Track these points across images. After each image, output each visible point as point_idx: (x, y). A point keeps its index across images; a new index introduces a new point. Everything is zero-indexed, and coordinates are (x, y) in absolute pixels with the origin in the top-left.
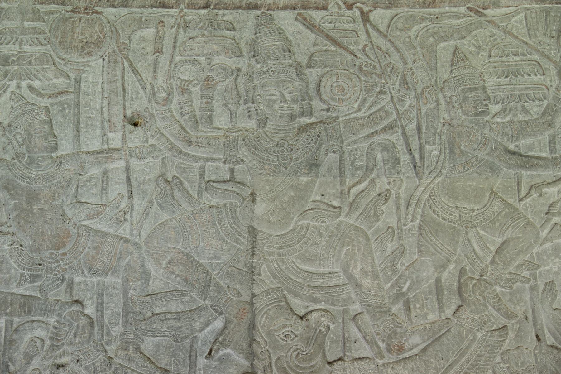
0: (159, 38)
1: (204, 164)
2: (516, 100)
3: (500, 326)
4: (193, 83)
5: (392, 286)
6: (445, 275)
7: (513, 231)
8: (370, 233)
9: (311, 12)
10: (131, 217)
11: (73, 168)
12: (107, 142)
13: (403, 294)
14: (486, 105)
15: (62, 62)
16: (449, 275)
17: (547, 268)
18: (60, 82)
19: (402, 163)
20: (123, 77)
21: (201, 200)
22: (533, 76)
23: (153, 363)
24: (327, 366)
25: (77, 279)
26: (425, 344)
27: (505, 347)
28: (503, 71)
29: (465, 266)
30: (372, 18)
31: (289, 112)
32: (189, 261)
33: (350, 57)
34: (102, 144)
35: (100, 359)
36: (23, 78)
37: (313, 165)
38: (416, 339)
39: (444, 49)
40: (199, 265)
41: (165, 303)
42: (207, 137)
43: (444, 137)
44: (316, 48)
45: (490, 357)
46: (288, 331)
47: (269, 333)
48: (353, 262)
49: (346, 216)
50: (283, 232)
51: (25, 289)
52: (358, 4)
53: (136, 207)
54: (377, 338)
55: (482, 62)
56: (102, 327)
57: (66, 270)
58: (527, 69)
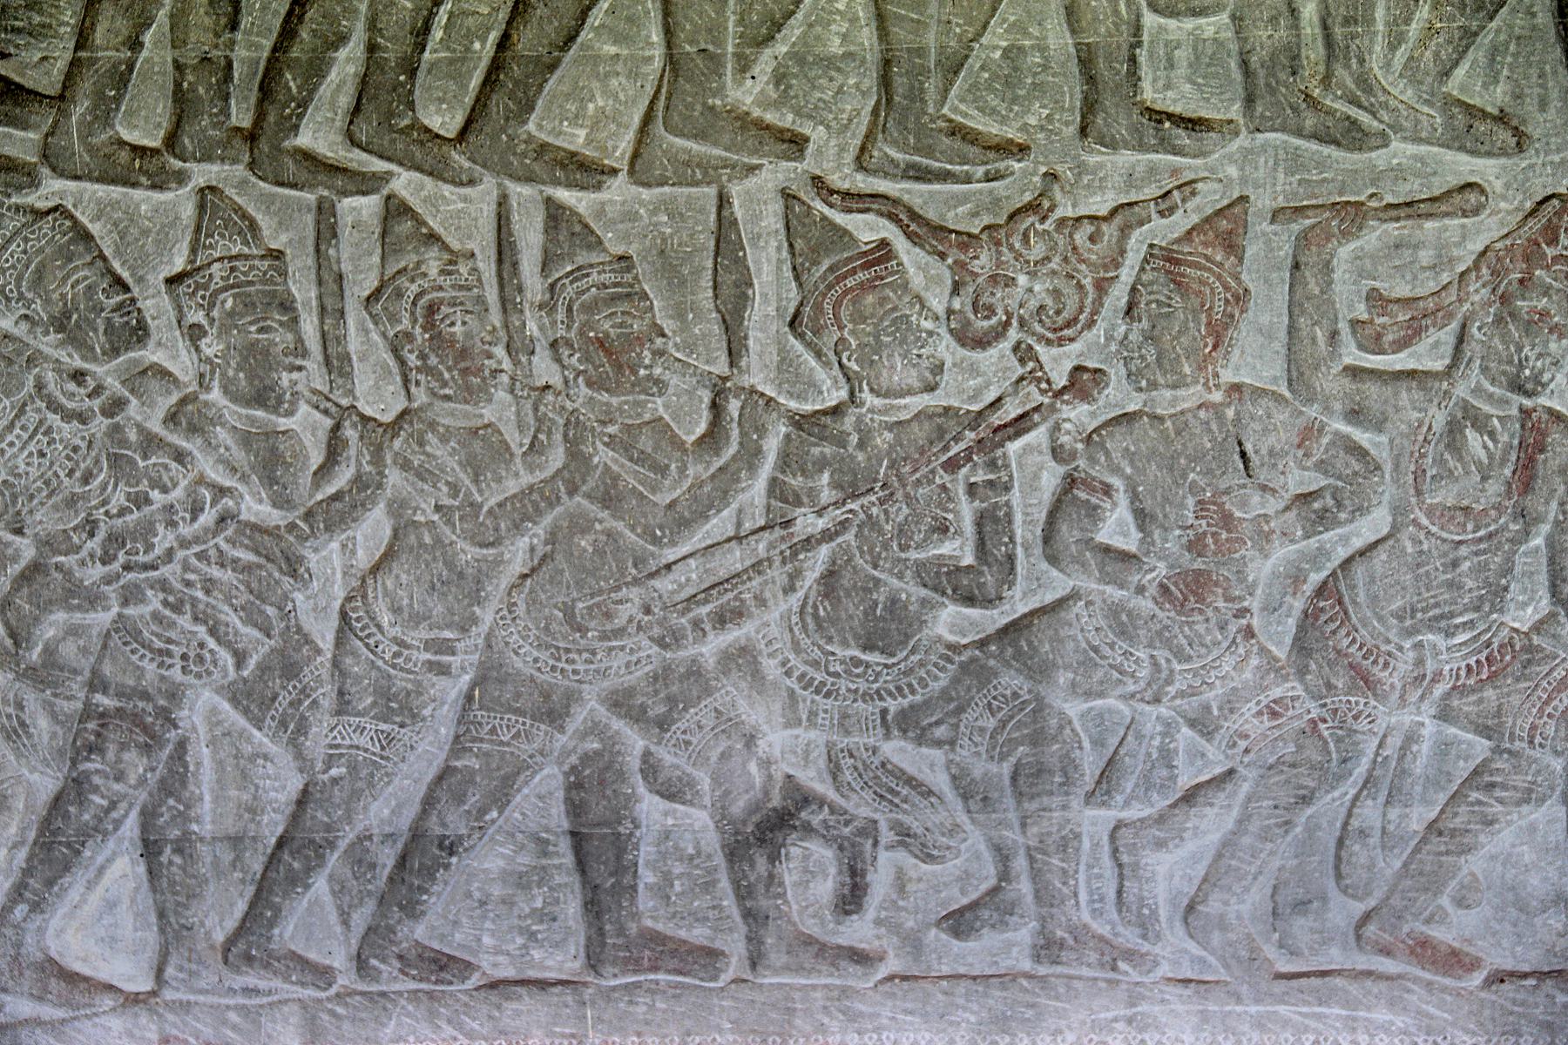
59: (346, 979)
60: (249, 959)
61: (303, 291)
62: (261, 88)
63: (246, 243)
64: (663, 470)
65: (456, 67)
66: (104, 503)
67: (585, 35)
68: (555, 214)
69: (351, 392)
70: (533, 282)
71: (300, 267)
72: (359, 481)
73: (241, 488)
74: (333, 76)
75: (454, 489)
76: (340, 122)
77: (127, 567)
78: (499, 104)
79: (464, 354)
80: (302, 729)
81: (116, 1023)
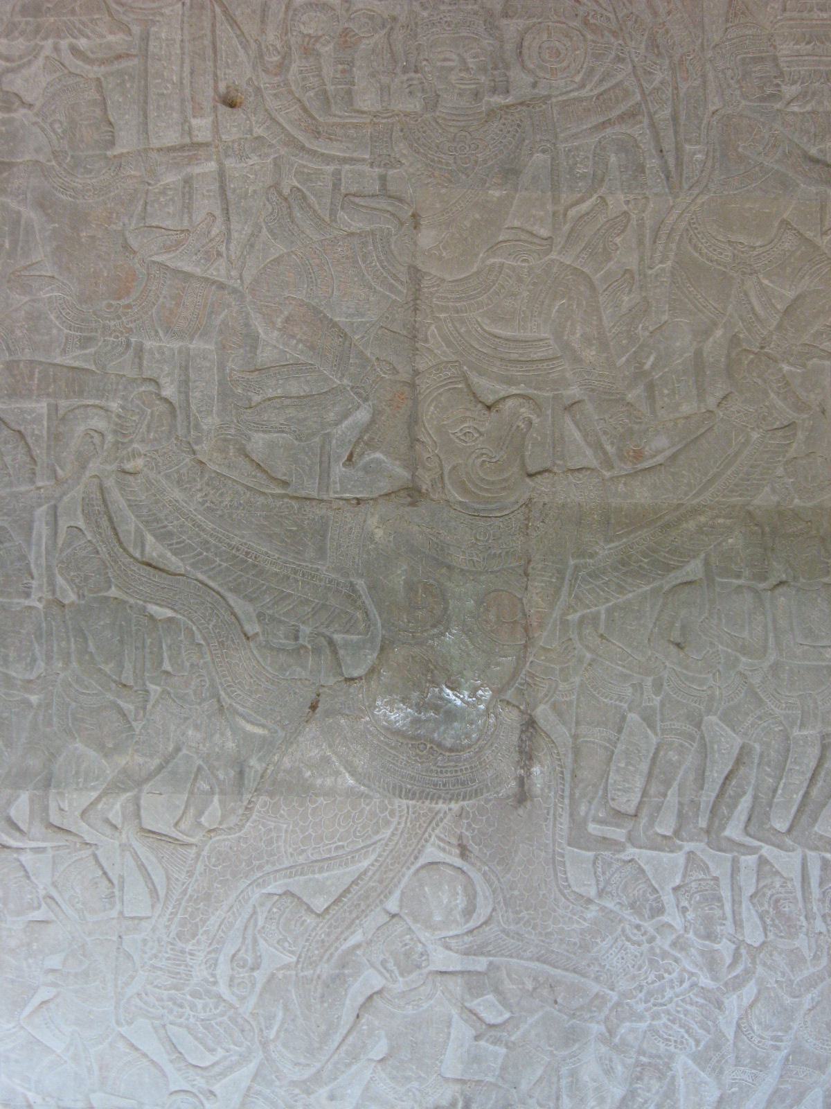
1: (339, 167)
2: (822, 80)
3: (786, 423)
4: (322, 40)
5: (628, 361)
6: (708, 346)
7: (812, 282)
8: (597, 278)
10: (228, 249)
11: (138, 174)
12: (190, 133)
14: (778, 85)
15: (121, 9)
19: (647, 172)
20: (213, 31)
21: (334, 224)
23: (264, 471)
24: (527, 480)
25: (148, 344)
26: (674, 450)
27: (791, 453)
28: (804, 34)
29: (739, 332)
31: (473, 86)
34: (182, 135)
35: (186, 464)
36: (62, 35)
37: (510, 172)
38: (662, 442)
40: (335, 325)
41: (281, 382)
42: (343, 126)
45: (769, 469)
46: (469, 427)
48: (569, 323)
49: (560, 253)
50: (462, 276)
51: (73, 358)
53: (235, 235)
54: (604, 438)
55: (772, 18)
56: (188, 417)
57: (131, 329)
61: (726, 893)
62: (711, 812)
63: (705, 874)
66: (646, 978)
69: (743, 935)
70: (816, 892)
71: (725, 884)
72: (747, 971)
73: (700, 973)
74: (739, 808)
75: (783, 974)
76: (742, 826)
77: (655, 1005)
78: (804, 819)
80: (721, 1072)
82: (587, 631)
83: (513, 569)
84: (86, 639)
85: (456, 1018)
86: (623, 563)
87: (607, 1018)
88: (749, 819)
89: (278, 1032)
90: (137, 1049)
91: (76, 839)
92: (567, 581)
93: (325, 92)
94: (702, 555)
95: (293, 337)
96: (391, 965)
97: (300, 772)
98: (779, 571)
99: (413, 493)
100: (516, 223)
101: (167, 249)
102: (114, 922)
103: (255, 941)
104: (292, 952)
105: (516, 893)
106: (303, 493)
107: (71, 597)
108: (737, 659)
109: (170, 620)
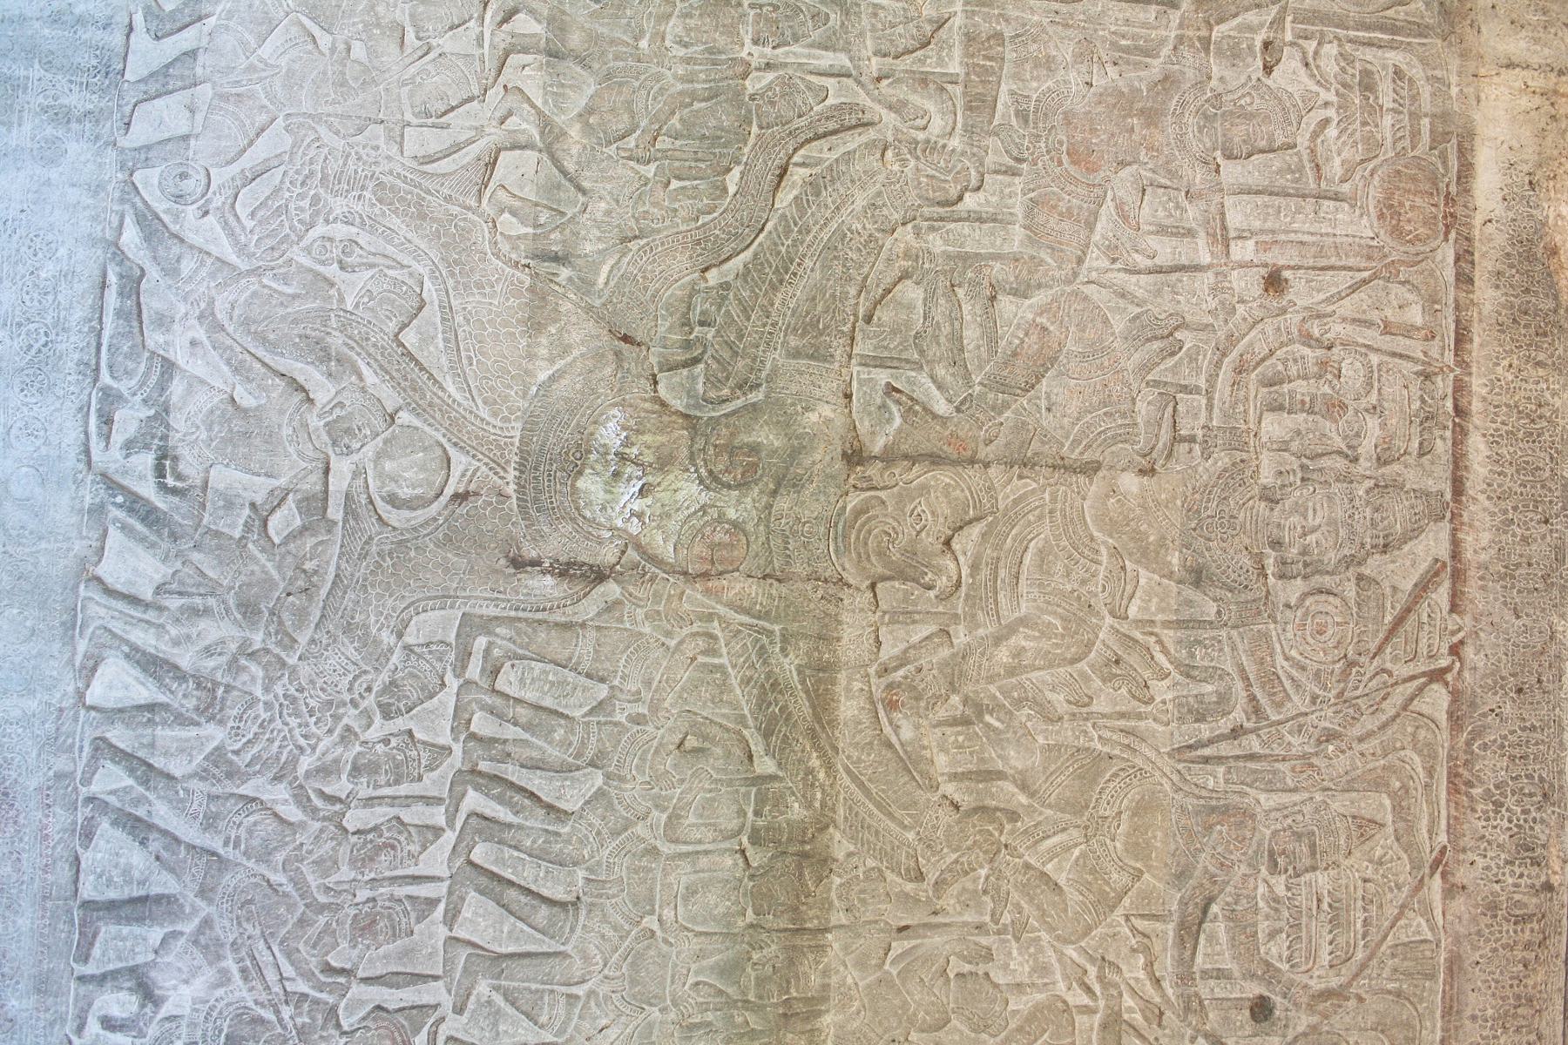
0: (1408, 331)
5: (995, 697)
6: (1009, 787)
8: (1083, 665)
9: (1447, 584)
10: (1119, 270)
11: (1197, 181)
12: (1240, 237)
13: (980, 715)
14: (1286, 871)
15: (1367, 173)
16: (1008, 793)
17: (1015, 953)
18: (1335, 168)
20: (1344, 268)
22: (1329, 948)
24: (868, 583)
26: (898, 747)
28: (1339, 901)
30: (1435, 686)
32: (1046, 362)
33: (1373, 647)
37: (1197, 577)
38: (907, 733)
39: (1380, 805)
43: (1237, 798)
44: (1388, 591)
47: (924, 489)
52: (1458, 664)
53: (1134, 278)
54: (911, 667)
56: (942, 219)
58: (1341, 940)
59: (84, 791)
60: (96, 749)
61: (404, 789)
64: (314, 947)
65: (499, 860)
67: (512, 919)
68: (432, 903)
72: (315, 810)
75: (310, 852)
76: (479, 810)
79: (372, 860)
80: (202, 779)
81: (71, 689)
82: (702, 643)
83: (771, 562)
84: (704, 100)
85: (275, 483)
86: (774, 685)
87: (267, 651)
88: (486, 819)
89: (270, 288)
90: (258, 135)
91: (491, 80)
92: (756, 622)
93: (1281, 383)
94: (781, 774)
95: (1026, 334)
96: (337, 412)
97: (555, 321)
98: (757, 857)
99: (855, 456)
100: (1142, 581)
101: (1120, 207)
102: (399, 116)
103: (372, 266)
104: (357, 306)
105: (412, 554)
106: (859, 336)
107: (750, 86)
108: (664, 810)
109: (725, 190)
